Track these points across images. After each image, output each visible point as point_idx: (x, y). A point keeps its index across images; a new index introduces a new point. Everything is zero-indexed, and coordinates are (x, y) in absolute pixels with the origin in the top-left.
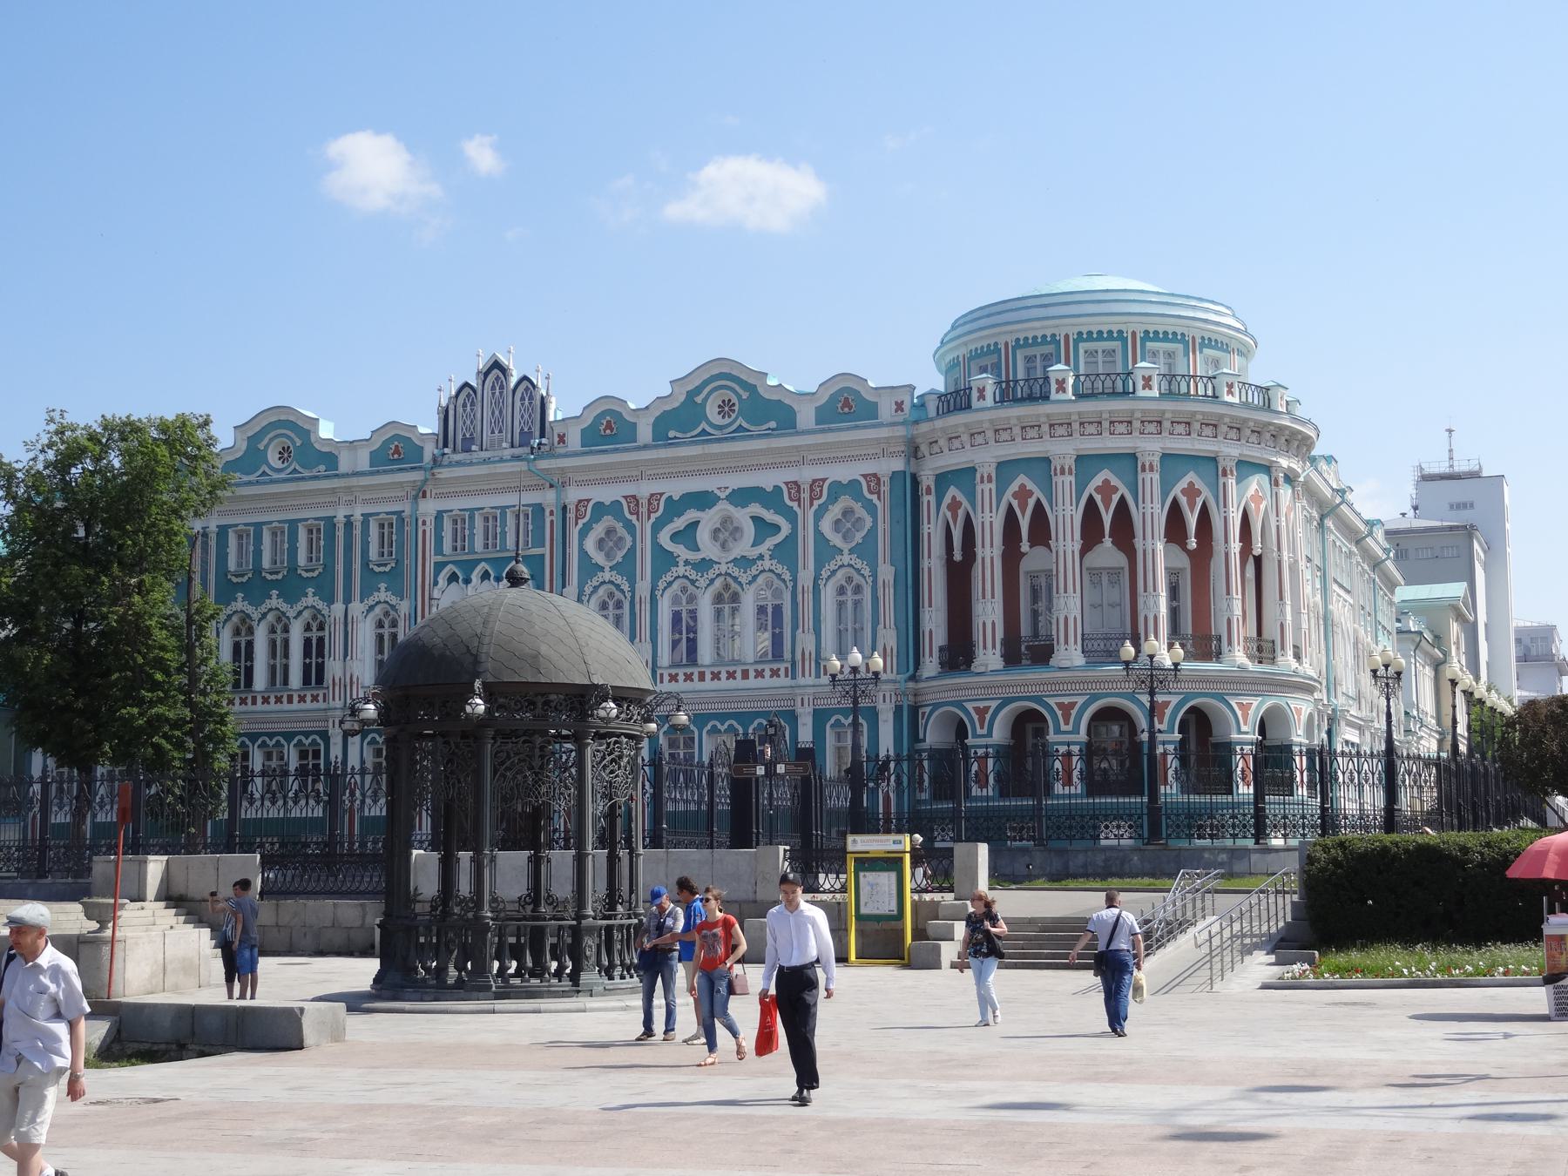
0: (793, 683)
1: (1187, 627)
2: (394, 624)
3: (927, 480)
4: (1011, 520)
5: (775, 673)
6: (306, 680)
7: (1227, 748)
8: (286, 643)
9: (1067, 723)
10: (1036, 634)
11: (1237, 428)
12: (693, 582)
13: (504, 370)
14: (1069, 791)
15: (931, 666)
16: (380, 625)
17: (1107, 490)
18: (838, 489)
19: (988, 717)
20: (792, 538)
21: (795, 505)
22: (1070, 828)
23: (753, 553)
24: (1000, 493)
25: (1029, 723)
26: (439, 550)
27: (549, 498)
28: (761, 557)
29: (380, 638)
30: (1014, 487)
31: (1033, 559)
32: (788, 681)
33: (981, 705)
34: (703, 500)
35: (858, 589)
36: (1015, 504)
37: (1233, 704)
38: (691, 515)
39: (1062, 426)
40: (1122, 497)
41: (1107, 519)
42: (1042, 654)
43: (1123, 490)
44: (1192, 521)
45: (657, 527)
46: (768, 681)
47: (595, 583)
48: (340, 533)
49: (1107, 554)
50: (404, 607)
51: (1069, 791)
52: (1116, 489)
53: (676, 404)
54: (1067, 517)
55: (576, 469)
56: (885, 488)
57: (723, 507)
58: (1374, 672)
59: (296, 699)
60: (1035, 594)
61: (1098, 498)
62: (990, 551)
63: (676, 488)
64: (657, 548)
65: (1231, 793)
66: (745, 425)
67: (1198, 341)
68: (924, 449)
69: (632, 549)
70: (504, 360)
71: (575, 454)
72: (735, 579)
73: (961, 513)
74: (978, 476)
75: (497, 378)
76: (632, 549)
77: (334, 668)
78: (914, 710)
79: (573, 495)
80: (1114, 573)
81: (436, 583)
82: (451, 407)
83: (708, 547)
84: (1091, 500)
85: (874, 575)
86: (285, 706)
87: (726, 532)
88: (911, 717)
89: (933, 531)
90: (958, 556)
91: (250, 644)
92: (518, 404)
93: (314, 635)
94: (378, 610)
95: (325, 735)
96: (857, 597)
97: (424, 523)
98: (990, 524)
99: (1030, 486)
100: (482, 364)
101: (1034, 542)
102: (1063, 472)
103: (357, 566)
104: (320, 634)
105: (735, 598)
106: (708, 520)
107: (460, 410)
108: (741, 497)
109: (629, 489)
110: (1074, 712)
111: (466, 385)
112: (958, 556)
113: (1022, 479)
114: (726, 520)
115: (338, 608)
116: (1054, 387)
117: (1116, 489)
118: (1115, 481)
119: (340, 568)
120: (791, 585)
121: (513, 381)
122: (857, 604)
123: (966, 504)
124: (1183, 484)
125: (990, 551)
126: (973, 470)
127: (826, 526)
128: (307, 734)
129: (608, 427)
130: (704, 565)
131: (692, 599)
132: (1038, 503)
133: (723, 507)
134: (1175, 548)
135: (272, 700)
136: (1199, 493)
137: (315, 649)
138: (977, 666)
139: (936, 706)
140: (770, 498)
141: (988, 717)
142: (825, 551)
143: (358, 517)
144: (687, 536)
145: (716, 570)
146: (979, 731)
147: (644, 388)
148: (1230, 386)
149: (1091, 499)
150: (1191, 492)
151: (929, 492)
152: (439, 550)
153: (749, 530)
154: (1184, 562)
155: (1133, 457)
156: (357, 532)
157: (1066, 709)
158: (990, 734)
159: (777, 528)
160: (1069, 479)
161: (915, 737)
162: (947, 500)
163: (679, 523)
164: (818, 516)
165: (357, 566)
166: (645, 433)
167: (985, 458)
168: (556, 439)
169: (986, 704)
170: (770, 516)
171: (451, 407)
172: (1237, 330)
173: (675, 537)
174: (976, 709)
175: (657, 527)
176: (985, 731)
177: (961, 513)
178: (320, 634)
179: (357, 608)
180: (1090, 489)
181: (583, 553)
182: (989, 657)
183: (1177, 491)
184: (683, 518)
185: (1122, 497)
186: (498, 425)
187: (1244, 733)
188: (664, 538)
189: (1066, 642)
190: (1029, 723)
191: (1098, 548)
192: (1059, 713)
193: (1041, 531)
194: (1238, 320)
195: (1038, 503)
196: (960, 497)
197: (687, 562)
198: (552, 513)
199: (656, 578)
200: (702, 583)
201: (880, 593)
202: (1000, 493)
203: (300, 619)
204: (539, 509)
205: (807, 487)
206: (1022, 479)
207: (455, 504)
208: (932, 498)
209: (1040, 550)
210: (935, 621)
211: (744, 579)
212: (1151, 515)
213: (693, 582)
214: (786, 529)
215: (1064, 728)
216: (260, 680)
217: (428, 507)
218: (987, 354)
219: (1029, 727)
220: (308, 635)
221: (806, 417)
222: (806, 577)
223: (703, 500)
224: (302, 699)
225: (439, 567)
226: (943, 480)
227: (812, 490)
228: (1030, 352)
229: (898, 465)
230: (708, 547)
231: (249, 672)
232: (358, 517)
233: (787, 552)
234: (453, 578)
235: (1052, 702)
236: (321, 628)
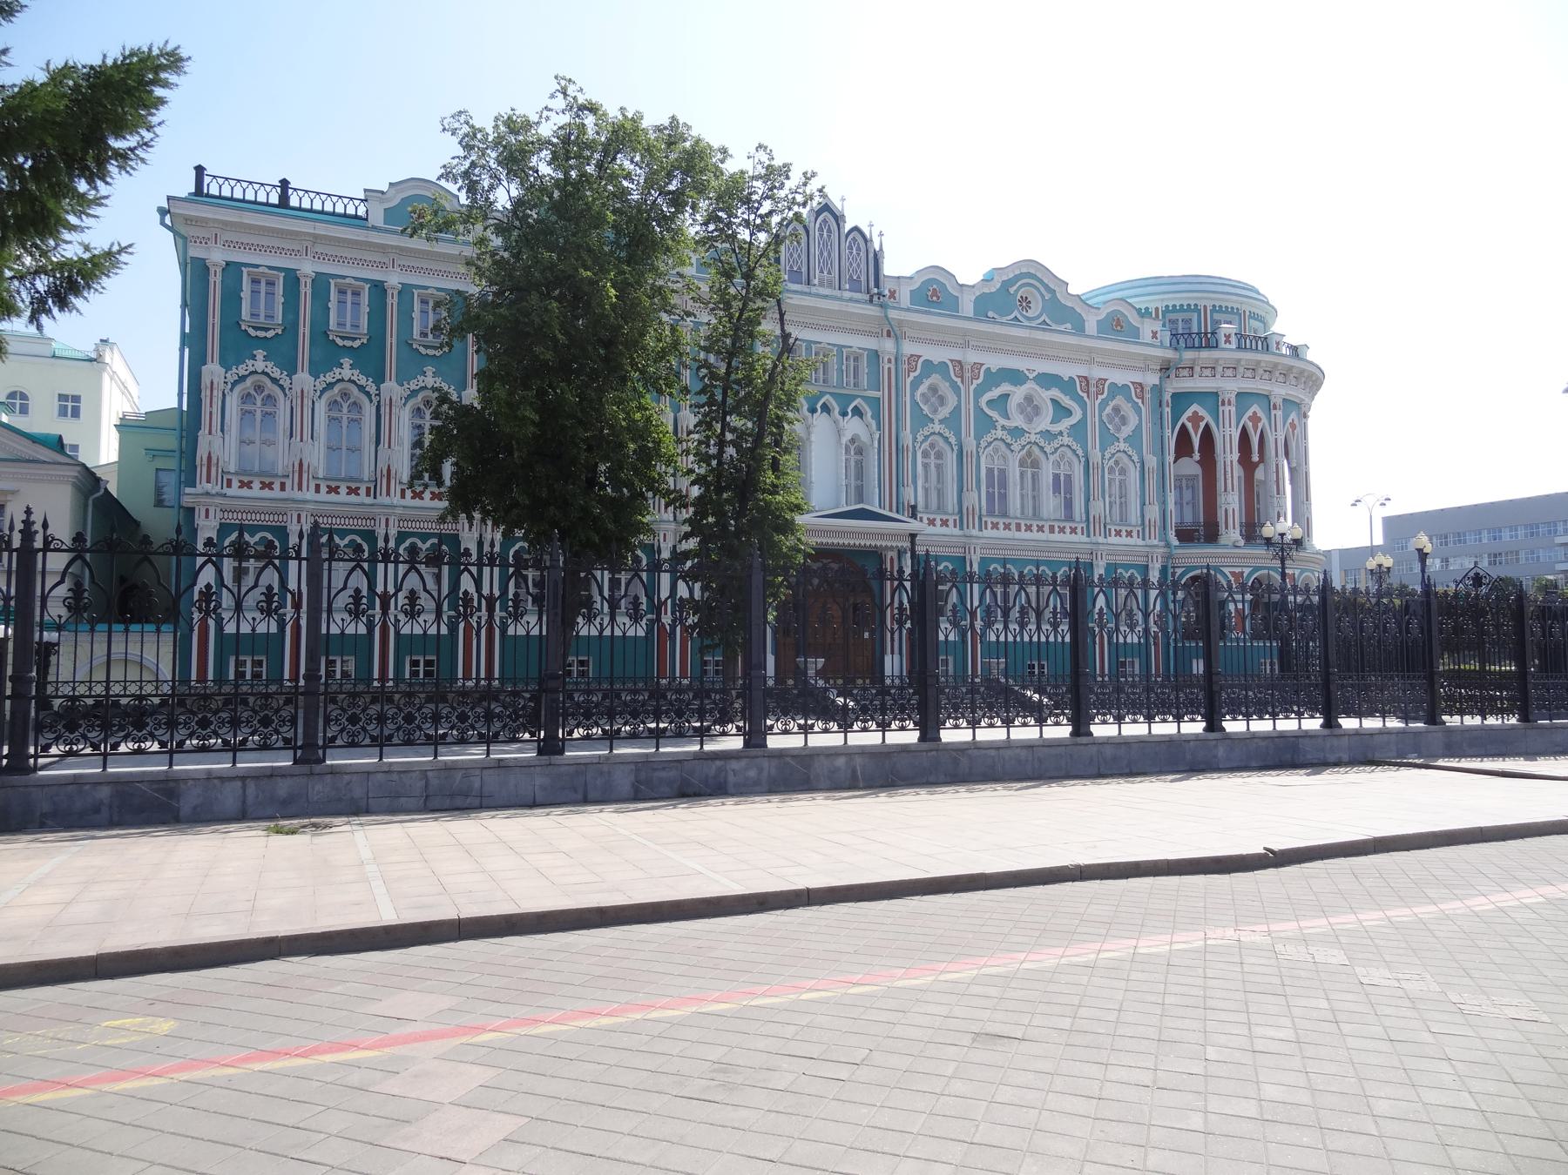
5: (1073, 531)
12: (1008, 445)
13: (839, 218)
18: (1116, 390)
20: (1082, 422)
23: (1055, 428)
27: (888, 346)
28: (1061, 433)
33: (1237, 570)
34: (1016, 377)
45: (979, 393)
46: (1068, 537)
55: (913, 325)
56: (1148, 396)
63: (995, 362)
64: (978, 409)
69: (958, 408)
72: (1042, 448)
73: (1202, 425)
75: (825, 221)
76: (958, 408)
79: (909, 348)
83: (1018, 421)
87: (1031, 408)
105: (1035, 464)
106: (1018, 394)
108: (1047, 380)
109: (956, 354)
113: (1255, 408)
114: (1029, 399)
121: (848, 227)
123: (1208, 419)
129: (935, 290)
130: (1017, 432)
138: (1223, 540)
140: (1067, 386)
153: (1049, 411)
159: (1069, 413)
166: (967, 308)
167: (1230, 387)
170: (1066, 401)
174: (1233, 573)
175: (979, 393)
181: (915, 403)
197: (1003, 427)
199: (978, 438)
200: (1016, 447)
204: (875, 355)
211: (1048, 449)
213: (1008, 445)
221: (1091, 326)
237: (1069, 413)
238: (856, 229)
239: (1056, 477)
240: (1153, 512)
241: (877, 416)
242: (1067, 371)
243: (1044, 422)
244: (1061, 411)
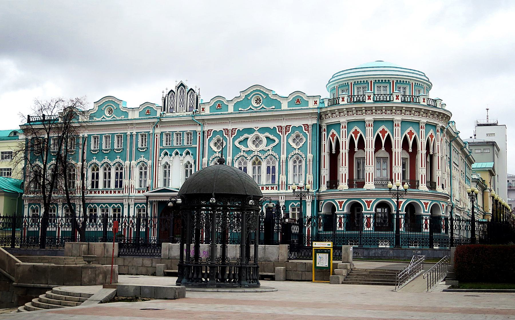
0: (279, 192)
1: (408, 177)
2: (146, 168)
3: (324, 127)
4: (352, 141)
5: (272, 188)
6: (116, 186)
7: (420, 217)
8: (110, 173)
9: (369, 207)
10: (358, 178)
11: (426, 112)
13: (184, 86)
14: (368, 230)
15: (324, 188)
16: (141, 169)
17: (383, 132)
19: (343, 204)
20: (279, 144)
21: (280, 133)
22: (370, 241)
24: (348, 132)
25: (356, 208)
26: (161, 144)
27: (199, 129)
28: (269, 150)
29: (187, 171)
30: (353, 130)
31: (358, 154)
32: (277, 191)
33: (341, 201)
34: (250, 131)
35: (300, 161)
36: (353, 135)
37: (422, 202)
38: (246, 135)
39: (369, 110)
40: (389, 134)
41: (383, 142)
42: (361, 185)
43: (389, 132)
44: (411, 143)
47: (252, 156)
48: (129, 138)
49: (383, 153)
50: (150, 163)
51: (368, 230)
52: (386, 132)
53: (242, 99)
54: (370, 140)
56: (310, 129)
57: (256, 133)
58: (469, 193)
59: (113, 192)
60: (358, 164)
61: (380, 135)
62: (344, 151)
63: (241, 127)
64: (234, 145)
65: (421, 232)
66: (264, 107)
67: (414, 84)
68: (323, 116)
70: (185, 83)
73: (335, 138)
74: (341, 126)
75: (182, 89)
77: (125, 182)
78: (318, 202)
79: (206, 129)
80: (385, 159)
81: (160, 156)
82: (166, 98)
84: (378, 134)
85: (306, 157)
86: (109, 195)
88: (317, 203)
89: (325, 143)
90: (334, 152)
91: (97, 174)
92: (189, 97)
93: (119, 171)
94: (140, 164)
95: (122, 204)
96: (300, 164)
97: (157, 136)
98: (344, 141)
99: (358, 130)
100: (178, 83)
101: (359, 148)
102: (369, 126)
103: (134, 149)
104: (121, 171)
105: (260, 163)
106: (251, 137)
107: (169, 99)
108: (263, 130)
110: (371, 204)
111: (172, 91)
112: (334, 152)
115: (127, 162)
116: (367, 98)
117: (386, 132)
118: (386, 129)
120: (278, 159)
121: (187, 90)
122: (300, 166)
123: (337, 135)
124: (408, 131)
125: (344, 151)
126: (340, 124)
127: (290, 141)
128: (116, 204)
129: (219, 104)
130: (249, 152)
131: (245, 163)
132: (361, 135)
133: (256, 133)
134: (405, 151)
135: (117, 192)
136: (413, 134)
137: (120, 176)
139: (325, 200)
140: (272, 131)
141: (343, 204)
143: (134, 133)
145: (254, 154)
146: (340, 209)
147: (230, 93)
148: (424, 99)
149: (378, 135)
150: (411, 133)
151: (324, 131)
153: (265, 141)
154: (407, 156)
155: (392, 121)
156: (134, 137)
158: (343, 210)
160: (371, 128)
161: (318, 210)
162: (331, 134)
165: (134, 149)
166: (231, 109)
168: (201, 109)
169: (342, 200)
170: (271, 137)
171: (166, 98)
172: (427, 81)
173: (240, 143)
176: (342, 209)
177: (335, 138)
178: (121, 171)
179: (134, 163)
180: (378, 131)
181: (210, 147)
182: (343, 186)
183: (406, 133)
184: (243, 137)
185: (389, 134)
186: (182, 104)
187: (425, 211)
188: (237, 143)
189: (369, 181)
190: (356, 208)
191: (380, 151)
192: (366, 204)
193: (362, 144)
194: (426, 77)
195: (361, 135)
197: (244, 151)
198: (199, 134)
200: (249, 158)
201: (308, 163)
202: (348, 132)
203: (115, 166)
205: (285, 128)
206: (356, 128)
207: (168, 130)
208: (326, 133)
209: (361, 151)
210: (325, 173)
212: (397, 141)
214: (277, 141)
215: (368, 209)
216: (101, 186)
217: (158, 131)
218: (343, 86)
219: (356, 208)
220: (117, 171)
221: (285, 106)
222: (283, 157)
223: (250, 131)
224: (115, 192)
225: (161, 150)
226: (330, 126)
227: (286, 129)
228: (359, 86)
229: (315, 122)
231: (97, 183)
232: (134, 133)
233: (277, 148)
234: (166, 154)
235: (364, 200)
236: (121, 169)
238: (191, 89)
239: (268, 168)
242: (271, 125)
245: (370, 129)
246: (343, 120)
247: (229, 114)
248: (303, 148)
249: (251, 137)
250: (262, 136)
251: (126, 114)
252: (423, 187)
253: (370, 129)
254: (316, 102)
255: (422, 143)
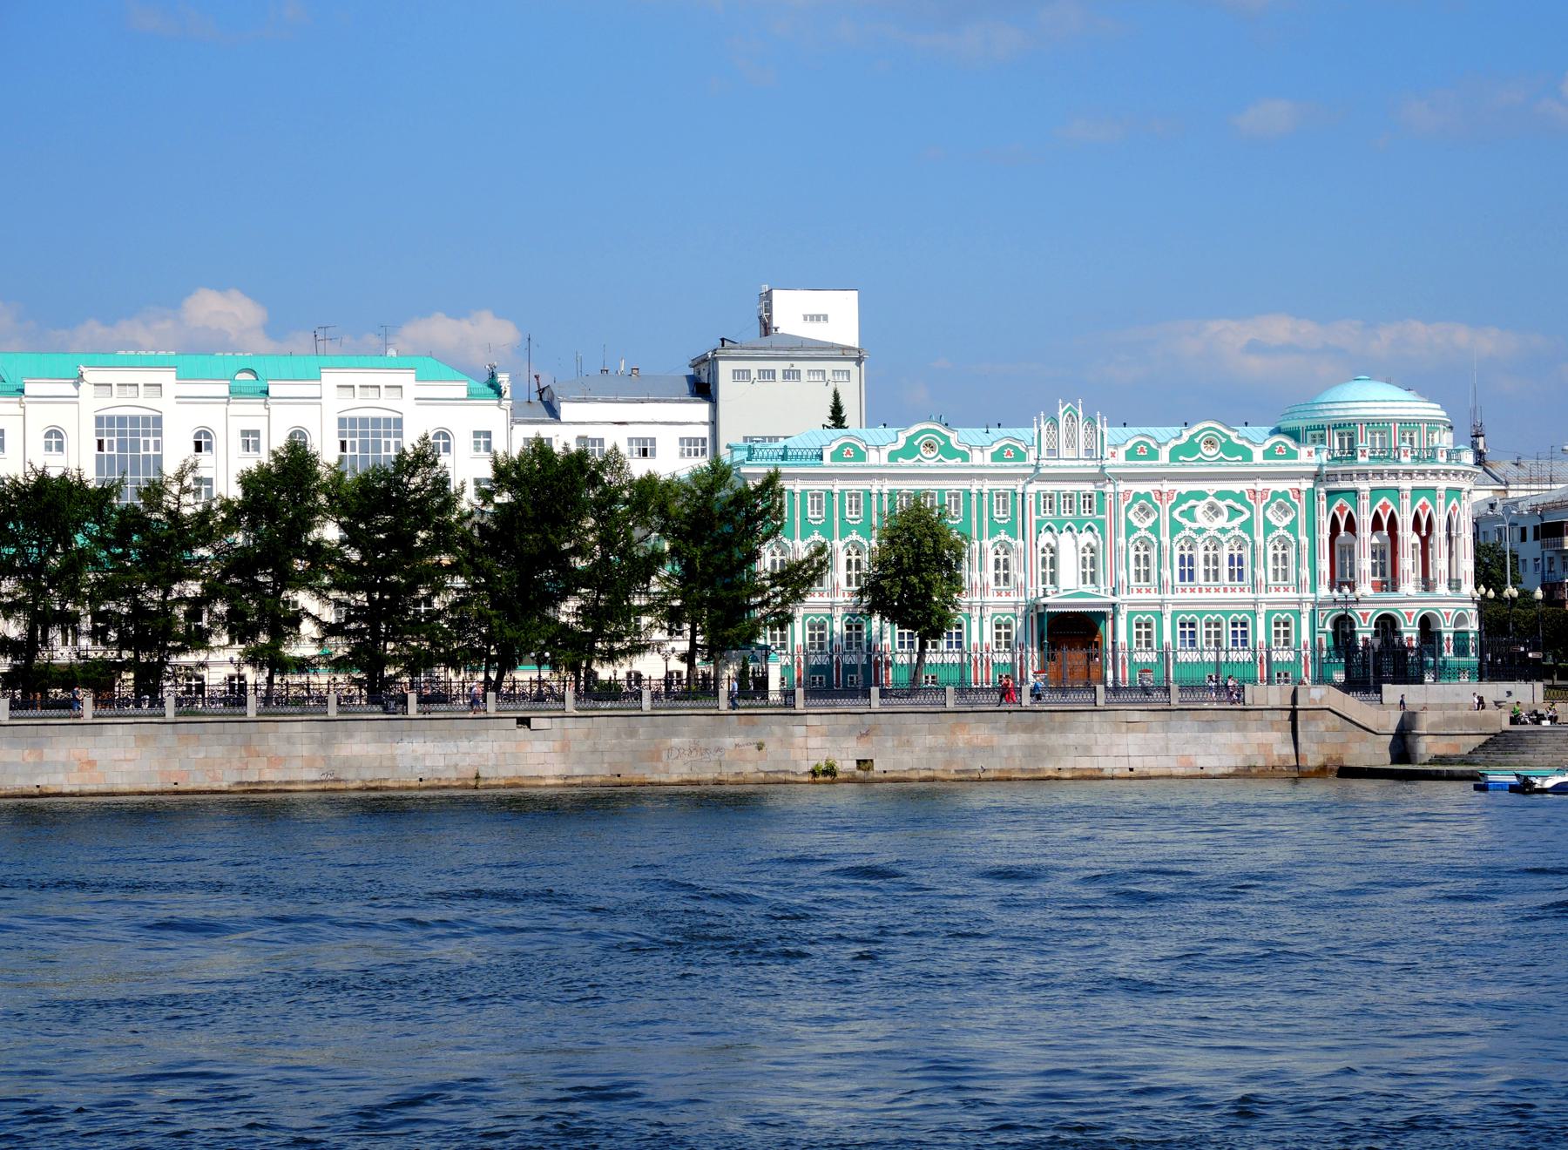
20: (1250, 520)
23: (1229, 526)
34: (1201, 495)
38: (1192, 502)
45: (1172, 509)
48: (974, 498)
56: (1303, 496)
57: (1210, 499)
63: (1184, 487)
64: (1172, 519)
71: (1167, 466)
83: (1202, 521)
98: (1365, 519)
103: (986, 519)
106: (1202, 506)
108: (1221, 495)
113: (1384, 499)
114: (1212, 507)
119: (974, 519)
127: (1269, 513)
130: (1200, 531)
140: (1239, 497)
142: (1269, 527)
144: (1189, 514)
152: (1038, 513)
153: (1225, 511)
156: (986, 498)
157: (1410, 615)
159: (1242, 513)
163: (1185, 507)
164: (1266, 507)
165: (986, 519)
170: (1238, 506)
175: (1172, 509)
181: (1128, 520)
188: (1176, 514)
196: (1346, 504)
200: (1199, 540)
211: (1224, 539)
214: (1247, 515)
217: (1032, 488)
230: (1202, 521)
232: (985, 490)
233: (1247, 526)
237: (1242, 513)
240: (1305, 573)
241: (1102, 532)
243: (1221, 521)
244: (1234, 512)
245: (1407, 502)
246: (1364, 486)
247: (1162, 466)
248: (1292, 528)
249: (1202, 506)
250: (1221, 504)
251: (965, 457)
252: (1442, 589)
253: (1407, 502)
254: (1310, 454)
255: (1405, 520)
